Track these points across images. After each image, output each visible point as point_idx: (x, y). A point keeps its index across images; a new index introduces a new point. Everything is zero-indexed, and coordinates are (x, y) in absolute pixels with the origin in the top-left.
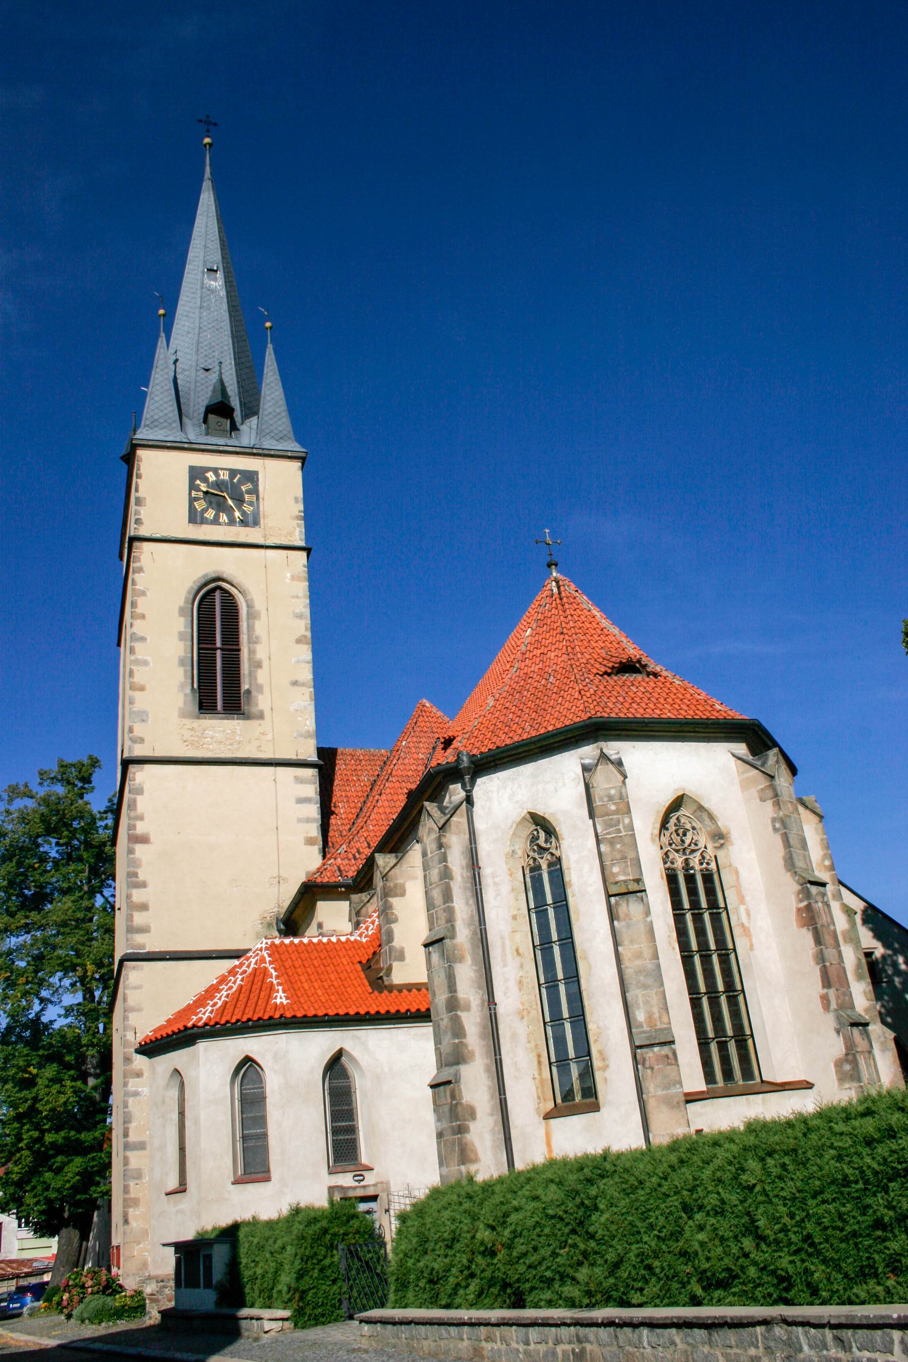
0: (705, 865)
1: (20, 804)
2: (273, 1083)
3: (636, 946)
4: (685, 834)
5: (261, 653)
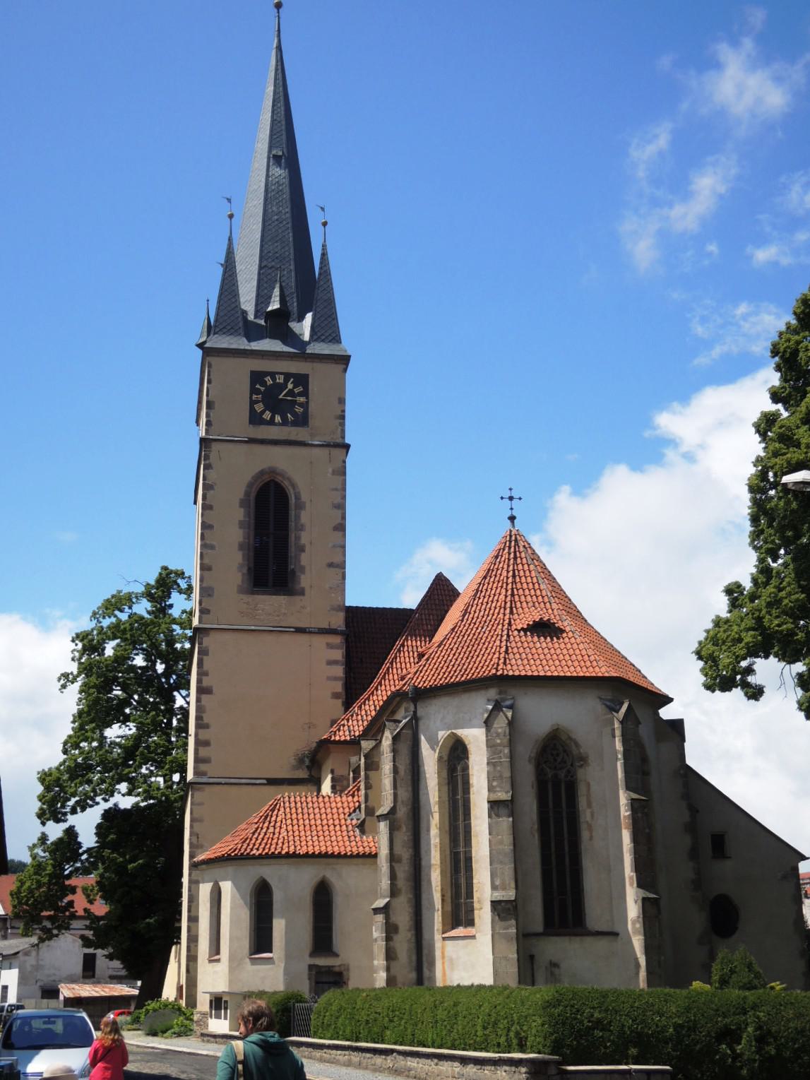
2: (277, 896)
3: (500, 837)
4: (558, 755)
5: (304, 539)
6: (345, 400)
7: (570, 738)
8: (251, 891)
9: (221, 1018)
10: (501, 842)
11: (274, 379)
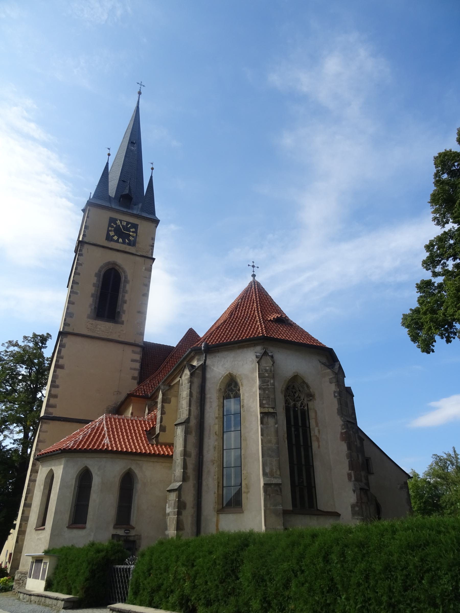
0: (302, 407)
1: (12, 349)
2: (96, 481)
3: (269, 437)
4: (295, 393)
5: (127, 297)
6: (155, 239)
7: (304, 382)
8: (77, 477)
9: (38, 579)
10: (270, 442)
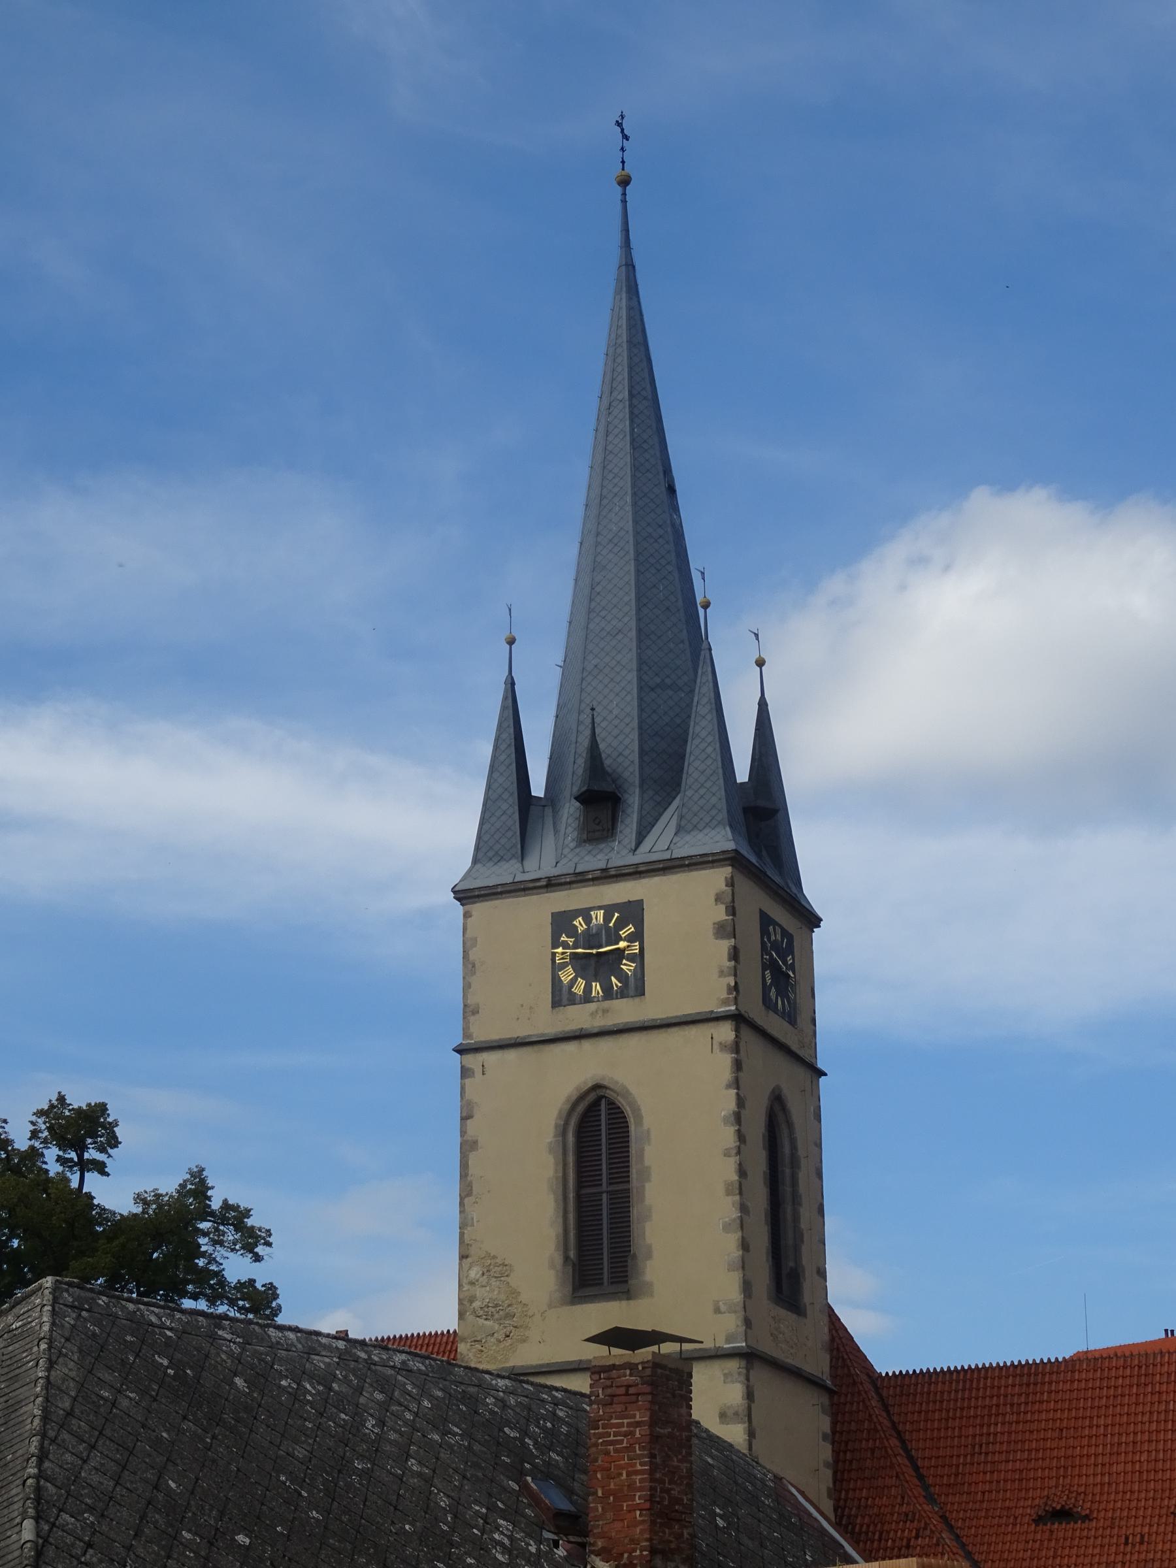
11: (588, 920)
